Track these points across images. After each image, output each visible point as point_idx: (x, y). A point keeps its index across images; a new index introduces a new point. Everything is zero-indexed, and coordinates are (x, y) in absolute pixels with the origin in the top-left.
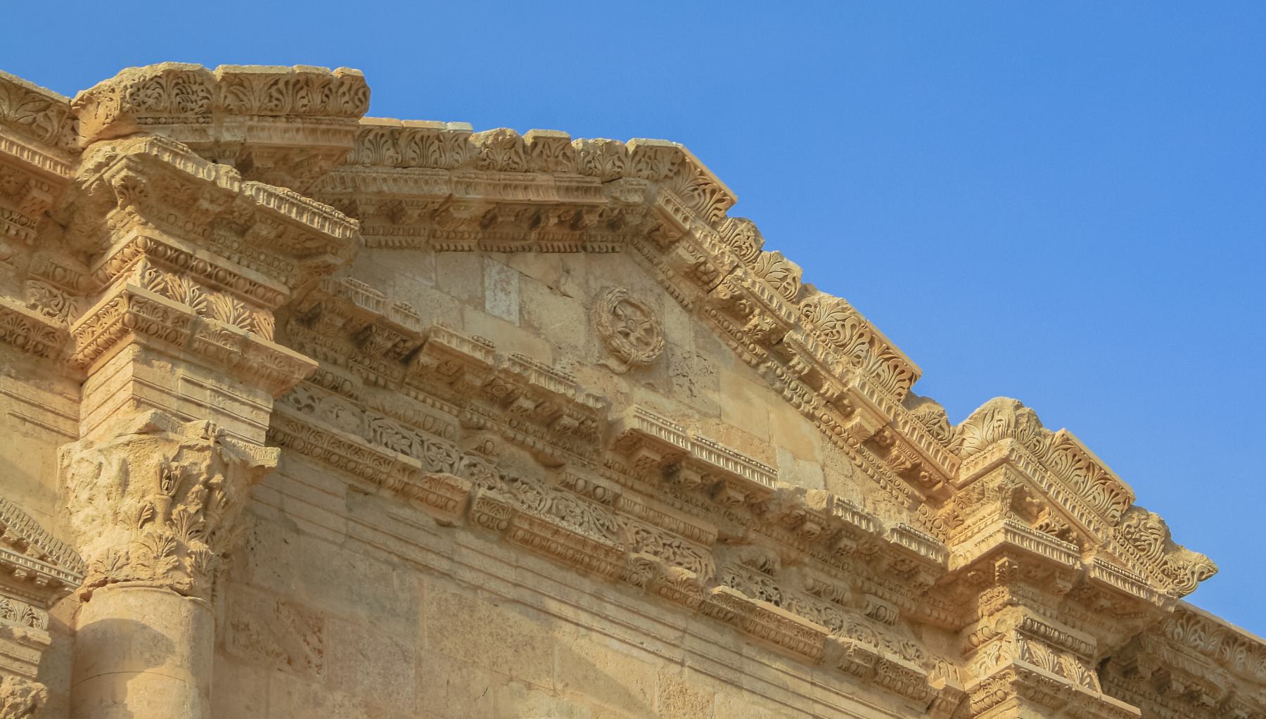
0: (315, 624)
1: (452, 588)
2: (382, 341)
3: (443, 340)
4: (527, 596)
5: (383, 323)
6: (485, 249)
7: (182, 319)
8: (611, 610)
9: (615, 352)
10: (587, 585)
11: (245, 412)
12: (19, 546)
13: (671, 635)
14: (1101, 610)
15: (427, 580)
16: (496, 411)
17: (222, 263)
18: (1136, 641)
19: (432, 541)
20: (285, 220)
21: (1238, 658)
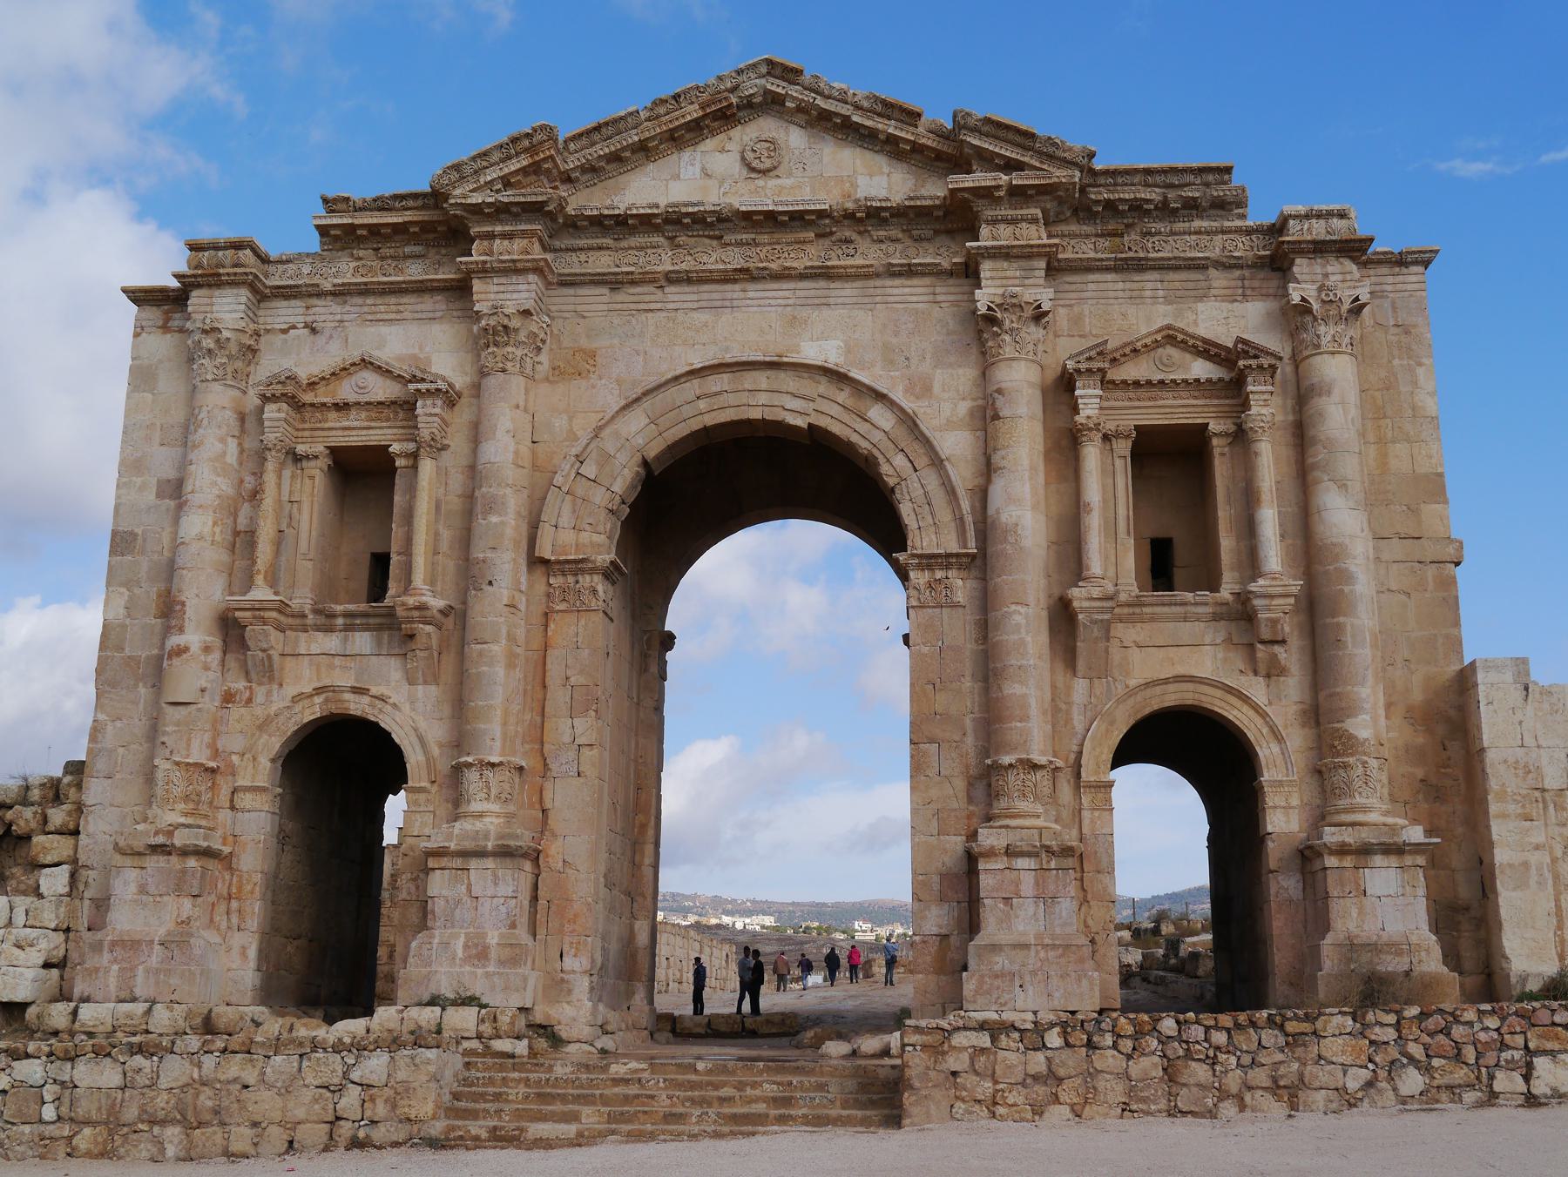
0: (592, 355)
1: (659, 313)
3: (634, 212)
4: (704, 304)
7: (485, 262)
8: (751, 294)
9: (753, 170)
10: (737, 287)
11: (524, 287)
12: (423, 380)
13: (787, 294)
14: (1031, 196)
15: (650, 315)
16: (677, 228)
17: (507, 228)
19: (652, 298)
21: (1159, 179)
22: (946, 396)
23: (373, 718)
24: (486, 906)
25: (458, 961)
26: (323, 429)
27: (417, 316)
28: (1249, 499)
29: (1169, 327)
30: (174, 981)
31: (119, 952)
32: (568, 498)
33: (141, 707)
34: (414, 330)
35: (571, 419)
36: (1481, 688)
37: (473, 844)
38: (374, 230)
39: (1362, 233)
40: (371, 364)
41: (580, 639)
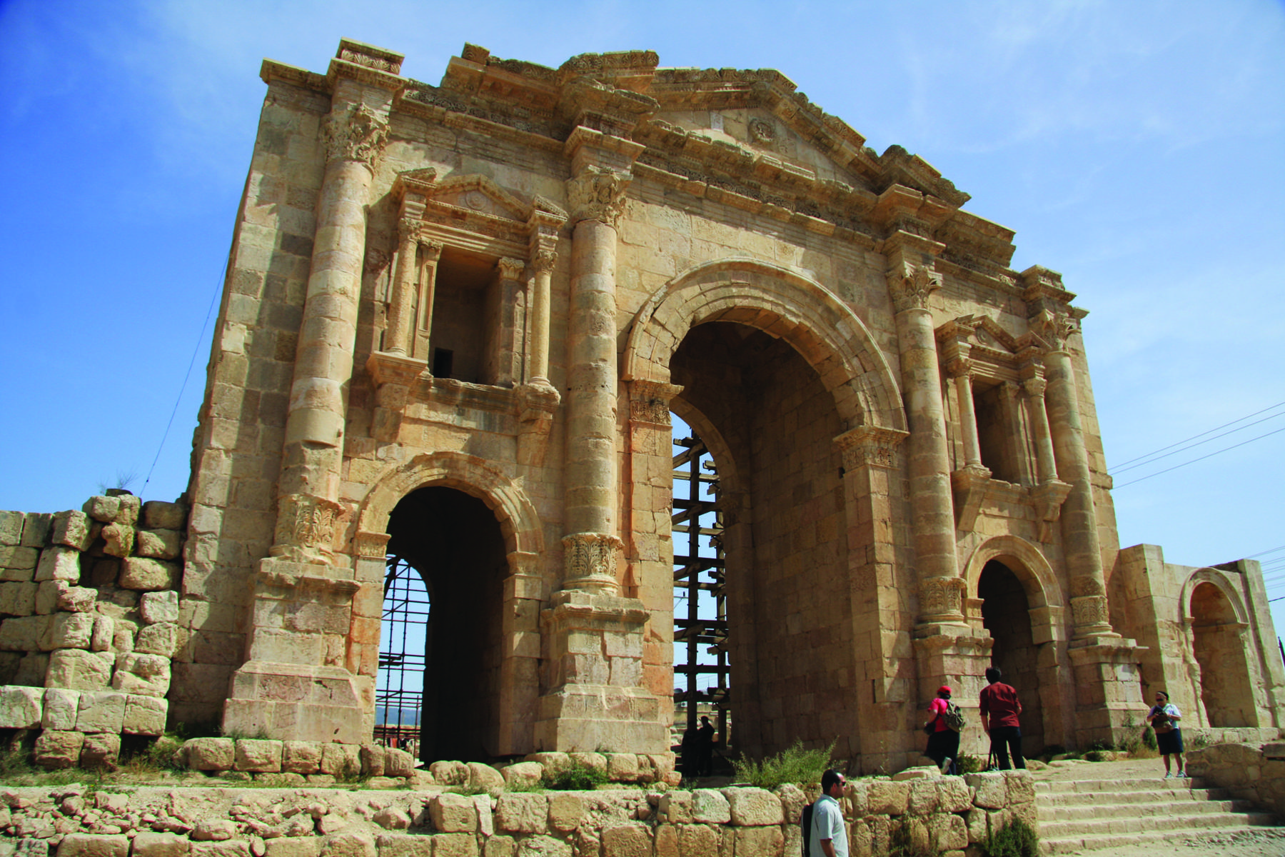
2: (672, 141)
5: (671, 134)
6: (710, 110)
12: (547, 211)
17: (612, 117)
18: (946, 224)
20: (632, 102)
22: (876, 326)
23: (485, 489)
24: (618, 664)
25: (604, 712)
26: (441, 230)
27: (519, 163)
28: (1036, 431)
29: (983, 318)
30: (337, 720)
31: (273, 687)
32: (645, 334)
33: (259, 441)
34: (517, 173)
35: (640, 275)
36: (1147, 561)
37: (610, 610)
38: (495, 87)
39: (1068, 289)
40: (484, 188)
41: (657, 448)
